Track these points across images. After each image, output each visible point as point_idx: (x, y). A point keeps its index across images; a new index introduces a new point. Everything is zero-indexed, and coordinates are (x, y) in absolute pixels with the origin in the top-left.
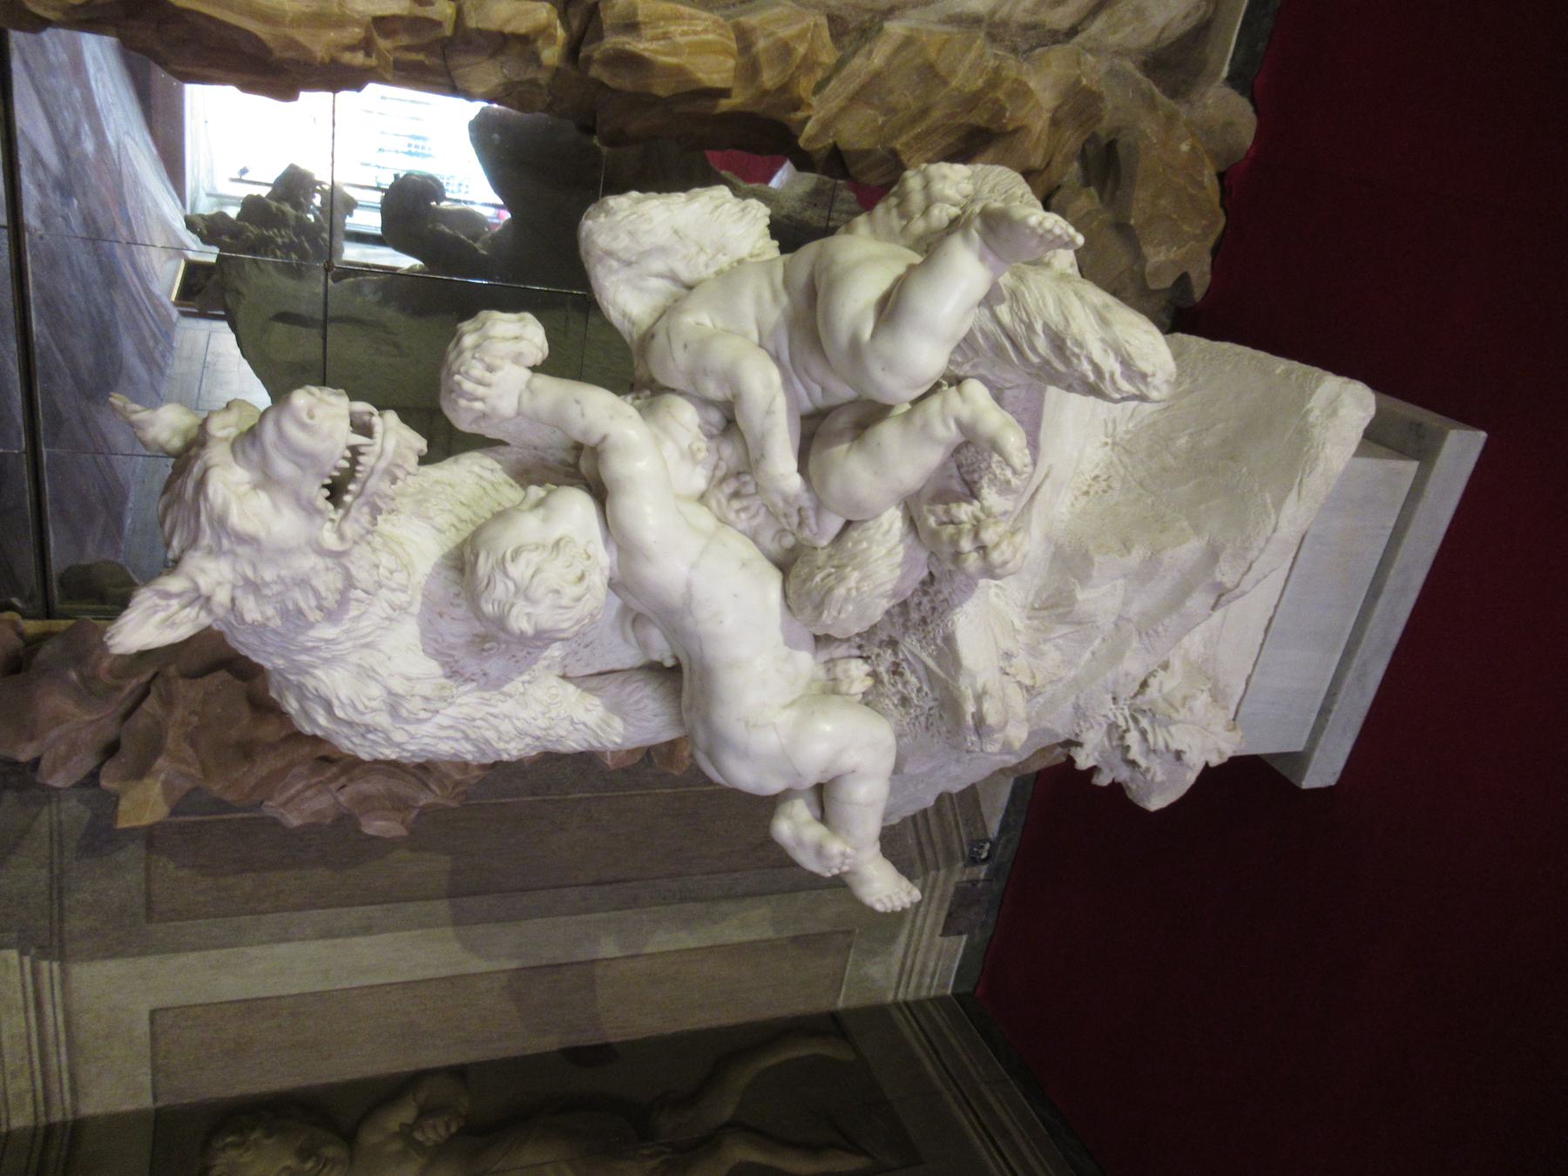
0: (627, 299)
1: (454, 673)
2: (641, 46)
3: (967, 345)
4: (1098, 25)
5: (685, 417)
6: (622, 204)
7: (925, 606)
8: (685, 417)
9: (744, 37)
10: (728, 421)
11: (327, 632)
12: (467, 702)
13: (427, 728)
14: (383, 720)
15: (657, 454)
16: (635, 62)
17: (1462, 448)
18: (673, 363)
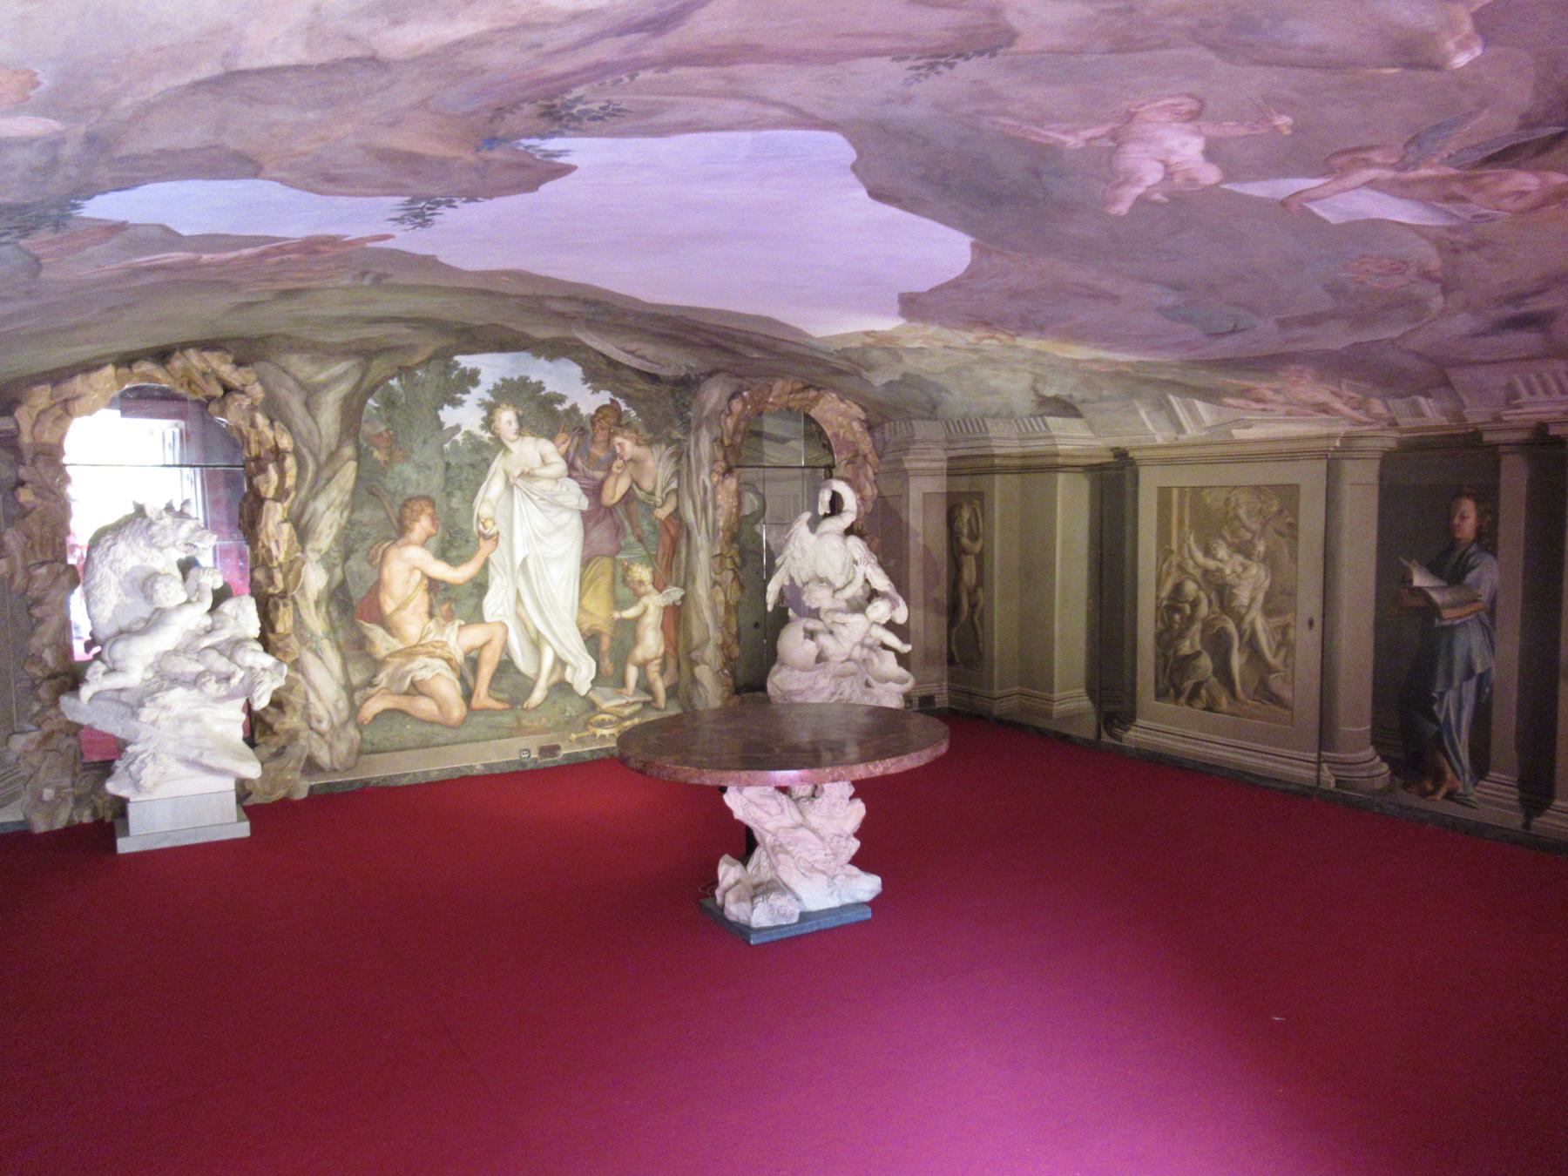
0: (228, 607)
1: (127, 574)
2: (281, 608)
3: (251, 668)
4: (315, 736)
5: (208, 621)
6: (253, 601)
7: (175, 681)
8: (208, 621)
9: (288, 636)
10: (209, 631)
11: (142, 543)
12: (114, 579)
13: (106, 569)
14: (111, 557)
15: (197, 616)
16: (277, 607)
17: (243, 830)
18: (216, 617)
